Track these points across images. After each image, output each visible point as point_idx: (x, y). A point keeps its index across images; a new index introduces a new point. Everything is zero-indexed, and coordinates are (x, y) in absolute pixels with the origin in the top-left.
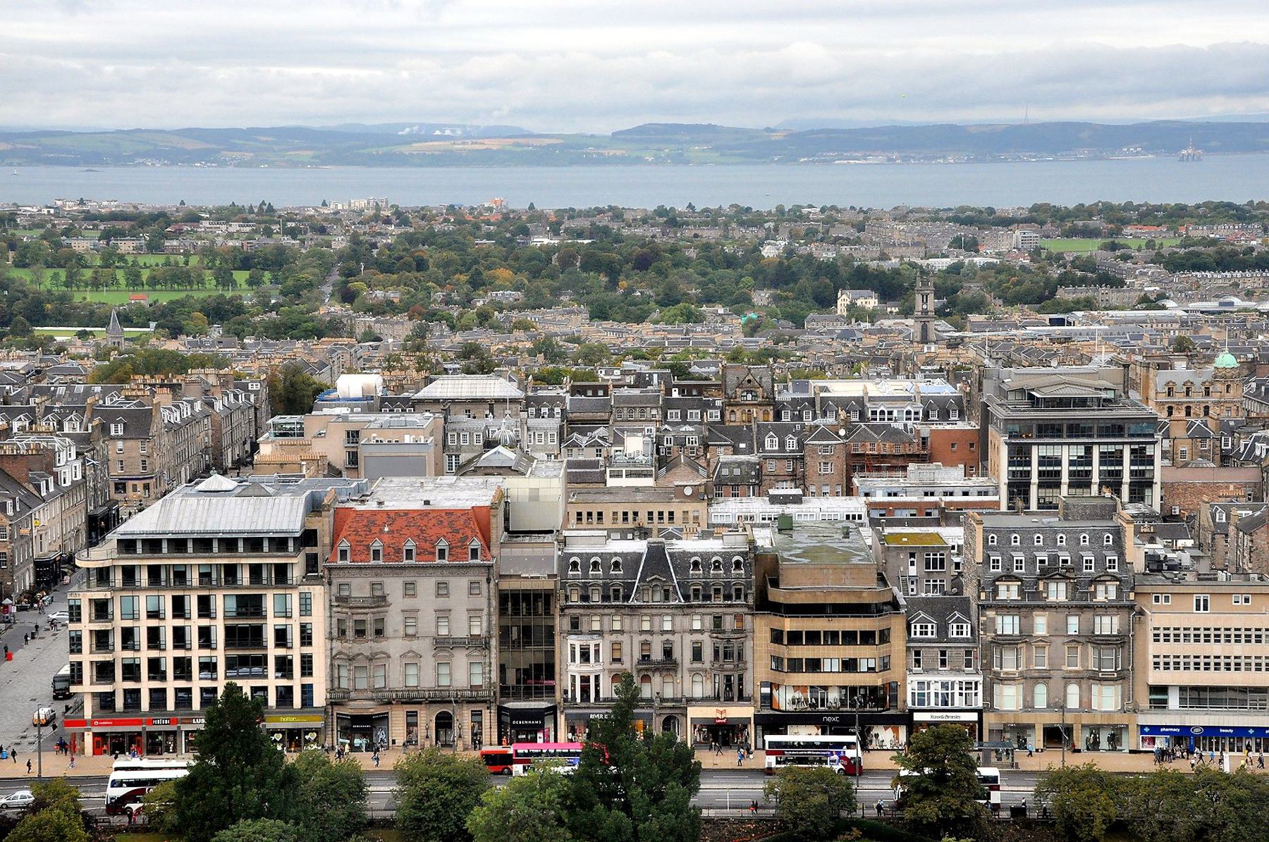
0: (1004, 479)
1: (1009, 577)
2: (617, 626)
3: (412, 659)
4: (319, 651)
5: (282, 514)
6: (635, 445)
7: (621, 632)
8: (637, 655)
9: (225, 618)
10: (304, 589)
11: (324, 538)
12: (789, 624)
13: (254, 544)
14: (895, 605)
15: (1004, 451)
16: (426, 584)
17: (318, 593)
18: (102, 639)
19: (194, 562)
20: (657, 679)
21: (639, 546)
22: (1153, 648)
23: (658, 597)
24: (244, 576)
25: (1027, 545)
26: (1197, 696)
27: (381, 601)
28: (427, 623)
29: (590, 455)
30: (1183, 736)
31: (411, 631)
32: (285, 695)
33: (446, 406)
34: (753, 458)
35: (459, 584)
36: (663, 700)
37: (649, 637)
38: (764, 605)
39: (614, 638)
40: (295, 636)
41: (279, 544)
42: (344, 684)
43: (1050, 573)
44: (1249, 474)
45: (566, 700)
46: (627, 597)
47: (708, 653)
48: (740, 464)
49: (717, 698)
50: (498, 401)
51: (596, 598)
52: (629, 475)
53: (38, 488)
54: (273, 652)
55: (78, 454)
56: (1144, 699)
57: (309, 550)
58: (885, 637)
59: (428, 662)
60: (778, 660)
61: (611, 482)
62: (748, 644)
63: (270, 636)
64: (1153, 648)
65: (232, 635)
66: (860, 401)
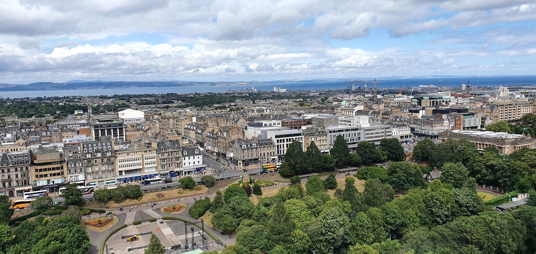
0: (94, 136)
1: (88, 153)
6: (9, 136)
12: (39, 168)
14: (65, 161)
15: (94, 131)
22: (119, 164)
25: (92, 147)
26: (127, 172)
30: (125, 180)
38: (33, 164)
43: (97, 151)
44: (142, 132)
56: (118, 174)
58: (62, 168)
60: (37, 176)
64: (118, 164)
66: (66, 125)
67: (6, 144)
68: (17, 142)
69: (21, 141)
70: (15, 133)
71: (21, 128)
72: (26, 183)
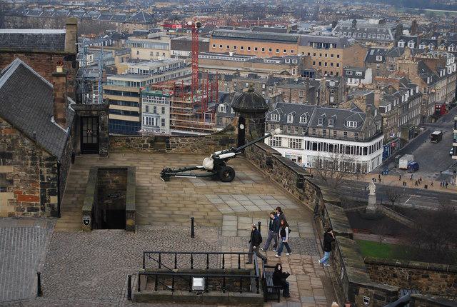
53: (439, 74)
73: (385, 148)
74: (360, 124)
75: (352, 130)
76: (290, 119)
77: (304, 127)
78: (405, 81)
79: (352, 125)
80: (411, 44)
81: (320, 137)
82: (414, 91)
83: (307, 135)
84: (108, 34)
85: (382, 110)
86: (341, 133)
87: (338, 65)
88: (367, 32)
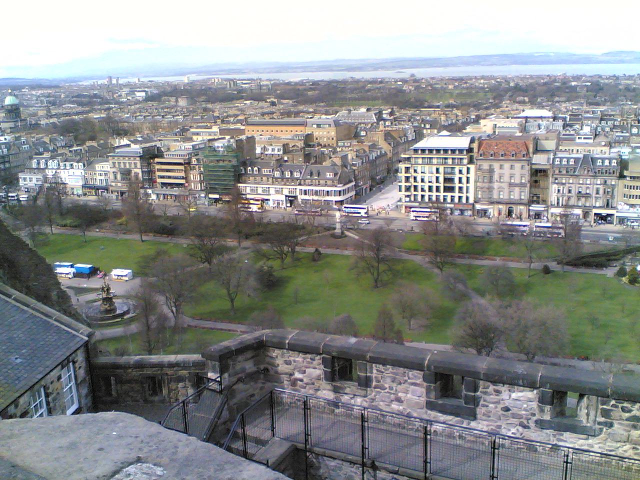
2: (571, 181)
3: (500, 190)
4: (472, 185)
5: (462, 142)
6: (587, 130)
7: (572, 183)
8: (577, 191)
9: (444, 174)
10: (469, 166)
11: (476, 150)
13: (453, 151)
16: (507, 165)
17: (472, 167)
18: (407, 179)
19: (434, 155)
20: (583, 199)
21: (581, 156)
23: (586, 172)
24: (450, 161)
27: (491, 171)
28: (506, 179)
29: (572, 132)
31: (502, 180)
32: (460, 198)
33: (526, 118)
34: (627, 134)
35: (518, 166)
36: (585, 206)
37: (581, 185)
38: (622, 176)
39: (570, 185)
40: (464, 180)
41: (461, 151)
42: (480, 196)
45: (552, 205)
46: (574, 172)
47: (601, 192)
48: (622, 136)
49: (603, 207)
50: (545, 118)
51: (564, 172)
52: (584, 138)
53: (401, 140)
54: (457, 185)
55: (414, 131)
57: (471, 154)
59: (506, 190)
61: (578, 141)
62: (616, 189)
63: (457, 180)
65: (446, 180)
67: (582, 141)
68: (598, 140)
69: (602, 140)
70: (594, 125)
71: (602, 119)
72: (608, 205)
73: (356, 191)
74: (335, 175)
75: (329, 179)
76: (287, 174)
77: (297, 179)
78: (373, 147)
79: (330, 175)
80: (388, 123)
81: (309, 185)
82: (381, 152)
83: (300, 184)
84: (179, 128)
85: (354, 165)
86: (322, 182)
87: (333, 139)
88: (359, 117)
